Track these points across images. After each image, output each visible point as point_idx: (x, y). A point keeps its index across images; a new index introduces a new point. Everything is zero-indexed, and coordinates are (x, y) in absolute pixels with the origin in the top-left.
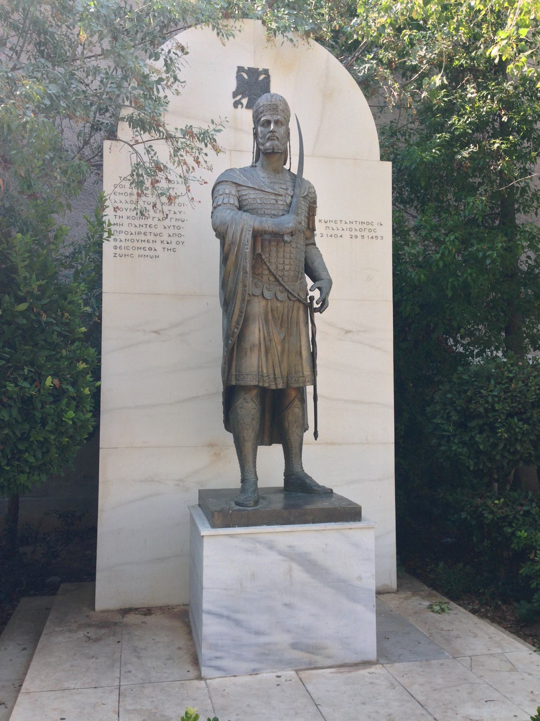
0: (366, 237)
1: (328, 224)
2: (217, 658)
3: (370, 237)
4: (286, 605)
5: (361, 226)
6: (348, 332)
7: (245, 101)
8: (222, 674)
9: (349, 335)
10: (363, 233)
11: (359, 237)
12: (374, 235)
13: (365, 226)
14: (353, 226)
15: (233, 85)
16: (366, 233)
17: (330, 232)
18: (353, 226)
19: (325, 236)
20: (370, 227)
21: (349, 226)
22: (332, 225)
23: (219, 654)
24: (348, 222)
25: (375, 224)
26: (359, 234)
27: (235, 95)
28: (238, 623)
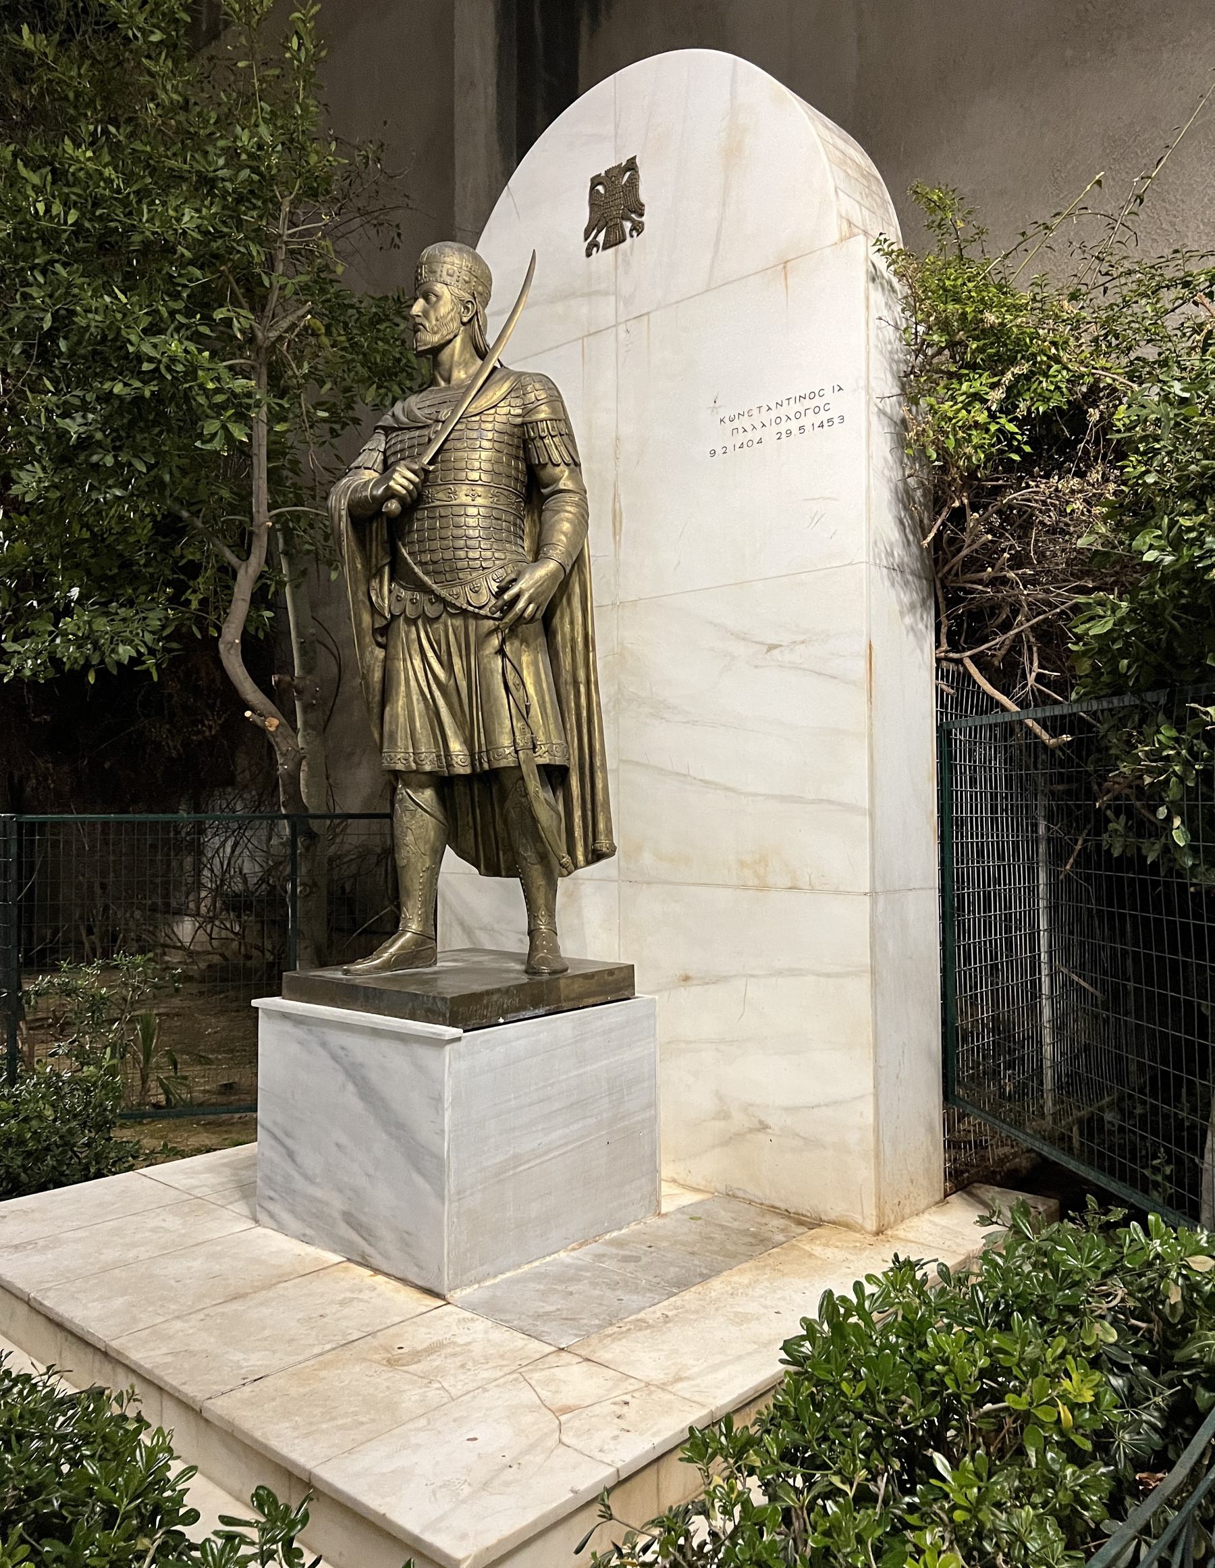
0: (808, 427)
1: (736, 424)
2: (271, 1198)
3: (816, 425)
4: (338, 1145)
5: (798, 407)
6: (772, 647)
7: (601, 238)
8: (273, 1224)
9: (776, 652)
10: (801, 422)
11: (795, 431)
12: (823, 416)
13: (807, 403)
14: (782, 412)
15: (583, 216)
16: (808, 420)
17: (741, 438)
18: (782, 412)
19: (730, 448)
20: (818, 401)
21: (773, 414)
22: (745, 422)
23: (272, 1194)
24: (773, 406)
25: (828, 392)
26: (794, 425)
27: (587, 236)
28: (291, 1155)
